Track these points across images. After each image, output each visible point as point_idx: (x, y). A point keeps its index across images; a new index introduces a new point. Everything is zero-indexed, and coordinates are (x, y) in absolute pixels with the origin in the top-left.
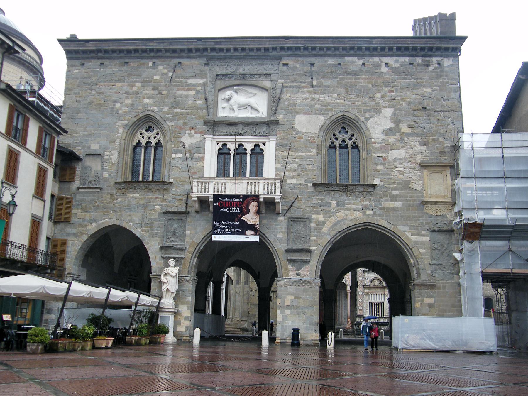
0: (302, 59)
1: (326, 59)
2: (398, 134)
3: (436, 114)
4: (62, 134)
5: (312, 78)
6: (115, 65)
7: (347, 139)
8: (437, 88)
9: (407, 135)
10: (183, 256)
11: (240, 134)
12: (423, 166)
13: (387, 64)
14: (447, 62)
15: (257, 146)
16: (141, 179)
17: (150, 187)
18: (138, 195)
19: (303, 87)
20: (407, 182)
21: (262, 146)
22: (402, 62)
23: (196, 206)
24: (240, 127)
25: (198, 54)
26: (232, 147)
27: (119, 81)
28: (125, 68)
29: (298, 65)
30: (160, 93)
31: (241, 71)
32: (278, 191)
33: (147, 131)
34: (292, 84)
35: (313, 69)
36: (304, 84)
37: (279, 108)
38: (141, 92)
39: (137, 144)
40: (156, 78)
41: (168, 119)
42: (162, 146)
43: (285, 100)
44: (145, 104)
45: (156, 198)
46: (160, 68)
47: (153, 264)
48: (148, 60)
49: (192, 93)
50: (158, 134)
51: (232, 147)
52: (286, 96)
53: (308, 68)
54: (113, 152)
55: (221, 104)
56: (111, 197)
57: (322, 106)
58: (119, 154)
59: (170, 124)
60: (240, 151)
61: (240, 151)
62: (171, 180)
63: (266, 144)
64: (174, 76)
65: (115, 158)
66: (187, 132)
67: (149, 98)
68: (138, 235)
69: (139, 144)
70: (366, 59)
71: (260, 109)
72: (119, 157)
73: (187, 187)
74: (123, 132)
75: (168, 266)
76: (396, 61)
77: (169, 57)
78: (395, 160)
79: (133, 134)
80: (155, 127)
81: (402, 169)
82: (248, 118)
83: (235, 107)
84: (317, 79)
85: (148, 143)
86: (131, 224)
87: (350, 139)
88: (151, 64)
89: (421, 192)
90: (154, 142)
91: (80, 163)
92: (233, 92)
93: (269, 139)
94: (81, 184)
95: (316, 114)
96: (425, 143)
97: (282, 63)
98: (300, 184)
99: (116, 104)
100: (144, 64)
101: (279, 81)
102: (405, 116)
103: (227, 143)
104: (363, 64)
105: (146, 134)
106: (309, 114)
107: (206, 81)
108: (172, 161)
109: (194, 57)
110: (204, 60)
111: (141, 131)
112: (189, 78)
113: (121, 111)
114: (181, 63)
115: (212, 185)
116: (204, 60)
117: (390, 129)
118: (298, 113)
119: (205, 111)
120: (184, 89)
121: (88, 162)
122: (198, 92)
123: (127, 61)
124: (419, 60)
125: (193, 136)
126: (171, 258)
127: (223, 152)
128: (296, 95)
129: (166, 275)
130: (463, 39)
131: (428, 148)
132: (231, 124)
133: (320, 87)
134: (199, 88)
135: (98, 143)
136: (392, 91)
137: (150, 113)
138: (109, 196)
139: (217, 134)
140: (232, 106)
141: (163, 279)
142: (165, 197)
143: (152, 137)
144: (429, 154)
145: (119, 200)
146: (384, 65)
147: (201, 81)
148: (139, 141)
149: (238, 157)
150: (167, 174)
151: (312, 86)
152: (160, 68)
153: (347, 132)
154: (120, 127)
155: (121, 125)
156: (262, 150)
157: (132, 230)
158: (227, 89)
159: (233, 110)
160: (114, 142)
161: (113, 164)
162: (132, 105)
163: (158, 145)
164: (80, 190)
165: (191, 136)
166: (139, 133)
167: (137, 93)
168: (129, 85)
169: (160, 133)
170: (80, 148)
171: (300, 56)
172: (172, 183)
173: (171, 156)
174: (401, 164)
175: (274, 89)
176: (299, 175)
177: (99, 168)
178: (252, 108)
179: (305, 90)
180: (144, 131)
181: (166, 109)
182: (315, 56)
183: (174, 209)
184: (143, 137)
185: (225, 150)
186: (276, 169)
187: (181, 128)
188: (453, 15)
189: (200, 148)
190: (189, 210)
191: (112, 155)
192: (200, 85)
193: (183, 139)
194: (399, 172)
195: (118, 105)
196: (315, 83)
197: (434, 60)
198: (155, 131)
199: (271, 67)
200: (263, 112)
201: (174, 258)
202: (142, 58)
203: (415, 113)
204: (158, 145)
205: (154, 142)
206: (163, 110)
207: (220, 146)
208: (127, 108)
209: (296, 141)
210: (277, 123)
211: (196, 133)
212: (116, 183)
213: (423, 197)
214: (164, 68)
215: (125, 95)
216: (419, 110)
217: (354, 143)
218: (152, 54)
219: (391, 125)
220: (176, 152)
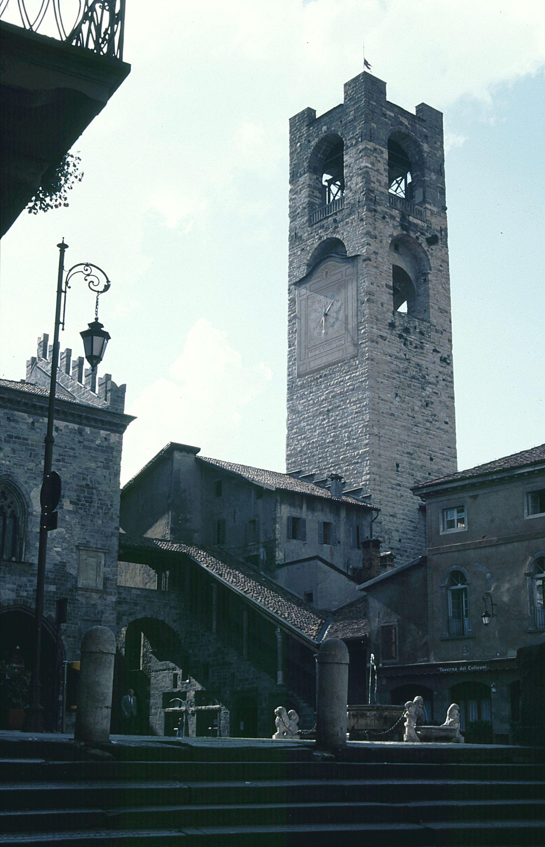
7: (6, 507)
14: (113, 437)
20: (63, 565)
22: (71, 429)
70: (36, 417)
81: (59, 549)
87: (9, 507)
89: (76, 579)
104: (33, 423)
124: (88, 430)
153: (6, 499)
188: (124, 387)
194: (57, 552)
213: (76, 582)
217: (13, 512)
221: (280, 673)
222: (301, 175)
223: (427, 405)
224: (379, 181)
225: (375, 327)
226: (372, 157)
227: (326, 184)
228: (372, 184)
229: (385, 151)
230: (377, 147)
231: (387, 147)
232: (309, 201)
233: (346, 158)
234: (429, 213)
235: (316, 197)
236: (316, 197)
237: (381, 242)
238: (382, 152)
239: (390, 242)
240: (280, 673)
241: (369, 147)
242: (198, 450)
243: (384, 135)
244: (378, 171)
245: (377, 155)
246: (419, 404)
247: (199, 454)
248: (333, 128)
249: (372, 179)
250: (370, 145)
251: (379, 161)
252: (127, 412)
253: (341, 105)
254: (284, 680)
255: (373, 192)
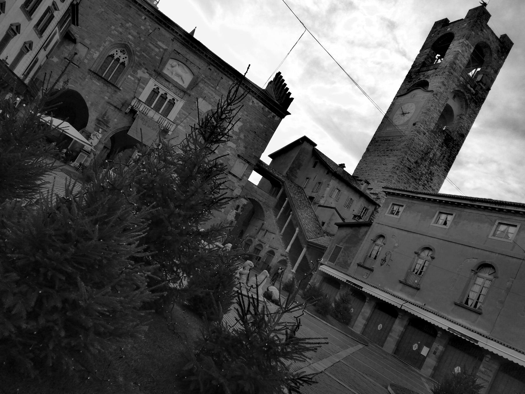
0: (219, 72)
1: (229, 80)
2: (238, 136)
3: (258, 138)
4: (75, 25)
5: (218, 85)
6: (123, 3)
8: (266, 127)
9: (241, 139)
10: (106, 130)
11: (169, 89)
12: (239, 156)
13: (253, 101)
14: (277, 118)
15: (174, 99)
16: (103, 76)
17: (108, 85)
18: (99, 84)
19: (211, 86)
21: (175, 101)
23: (128, 111)
24: (171, 85)
25: (171, 31)
26: (161, 92)
27: (120, 14)
28: (128, 9)
29: (215, 74)
30: (140, 37)
31: (187, 57)
32: (172, 130)
33: (121, 51)
34: (207, 81)
35: (221, 81)
36: (212, 85)
37: (194, 89)
38: (130, 30)
39: (111, 55)
40: (142, 27)
41: (137, 55)
42: (125, 66)
43: (199, 87)
44: (128, 38)
45: (108, 92)
46: (148, 24)
47: (88, 124)
48: (143, 15)
49: (157, 50)
50: (126, 58)
51: (161, 92)
52: (201, 85)
53: (219, 79)
54: (96, 52)
55: (168, 66)
56: (82, 76)
57: (214, 101)
58: (99, 56)
59: (136, 58)
60: (164, 97)
61: (164, 97)
62: (121, 88)
63: (179, 102)
64: (152, 33)
65: (96, 55)
66: (143, 69)
67: (132, 36)
68: (88, 104)
69: (112, 56)
71: (185, 82)
72: (98, 57)
73: (128, 97)
74: (108, 44)
75: (98, 131)
76: (257, 103)
77: (155, 21)
78: (230, 147)
79: (113, 48)
80: (126, 52)
82: (177, 83)
83: (174, 73)
84: (220, 87)
85: (118, 60)
86: (87, 97)
88: (143, 18)
90: (121, 60)
91: (74, 45)
92: (177, 65)
93: (181, 100)
94: (68, 56)
95: (210, 103)
96: (246, 148)
97: (208, 67)
98: (183, 131)
99: (112, 26)
100: (139, 15)
101: (202, 75)
102: (246, 130)
103: (160, 89)
105: (120, 54)
106: (206, 101)
107: (167, 49)
108: (127, 79)
109: (168, 31)
110: (172, 37)
111: (117, 49)
112: (160, 41)
113: (112, 32)
114: (160, 29)
115: (142, 107)
116: (172, 37)
117: (236, 132)
118: (202, 97)
119: (158, 64)
120: (154, 45)
121: (79, 46)
122: (160, 51)
123: (131, 6)
124: (267, 109)
125: (145, 73)
126: (100, 128)
127: (155, 92)
128: (206, 88)
129: (94, 135)
130: (289, 114)
131: (246, 150)
132: (167, 80)
133: (219, 92)
134: (161, 50)
135: (90, 41)
136: (247, 116)
137: (128, 44)
138: (82, 74)
139: (157, 80)
140: (173, 71)
141: (92, 136)
142: (113, 95)
143: (123, 58)
144: (244, 153)
145: (87, 80)
146: (251, 101)
147: (165, 47)
148: (114, 54)
149: (161, 98)
150: (120, 84)
151: (216, 89)
152: (148, 24)
154: (108, 40)
155: (109, 40)
156: (175, 103)
157: (86, 101)
158: (175, 60)
159: (172, 73)
160: (100, 47)
161: (93, 59)
162: (121, 33)
163: (123, 64)
164: (66, 60)
165: (144, 73)
166: (115, 50)
167: (127, 28)
168: (125, 21)
169: (127, 58)
170: (78, 36)
171: (219, 70)
172: (121, 90)
173: (128, 76)
174: (231, 150)
175: (197, 78)
176: (185, 126)
177: (84, 55)
178: (182, 78)
179: (212, 88)
180: (119, 51)
181: (138, 49)
182: (225, 75)
183: (115, 104)
184: (117, 54)
185: (156, 91)
186: (176, 116)
187: (141, 64)
188: (292, 99)
189: (146, 82)
190: (123, 109)
191: (96, 53)
192: (163, 48)
193: (139, 71)
195: (113, 27)
196: (218, 88)
197: (273, 114)
198: (125, 55)
199: (203, 65)
200: (185, 85)
201: (102, 129)
202: (140, 10)
203: (251, 132)
204: (123, 64)
205: (121, 60)
206: (136, 48)
207: (155, 87)
208: (117, 33)
209: (193, 110)
210: (190, 95)
211: (147, 72)
212: (90, 70)
213: (231, 169)
214: (150, 26)
215: (120, 25)
216: (252, 131)
218: (147, 13)
219: (238, 131)
220: (131, 75)
221: (289, 247)
222: (426, 49)
223: (430, 173)
224: (461, 61)
225: (423, 127)
226: (464, 48)
227: (437, 58)
228: (457, 61)
229: (473, 48)
230: (470, 44)
231: (474, 46)
232: (424, 61)
233: (451, 45)
234: (480, 87)
235: (428, 61)
236: (428, 61)
237: (447, 89)
238: (471, 48)
239: (451, 91)
240: (289, 247)
241: (465, 42)
242: (316, 145)
243: (476, 41)
244: (463, 56)
245: (467, 48)
246: (426, 171)
247: (316, 147)
248: (453, 30)
249: (459, 58)
250: (467, 42)
251: (467, 52)
252: (288, 110)
253: (462, 19)
254: (290, 251)
255: (455, 64)
